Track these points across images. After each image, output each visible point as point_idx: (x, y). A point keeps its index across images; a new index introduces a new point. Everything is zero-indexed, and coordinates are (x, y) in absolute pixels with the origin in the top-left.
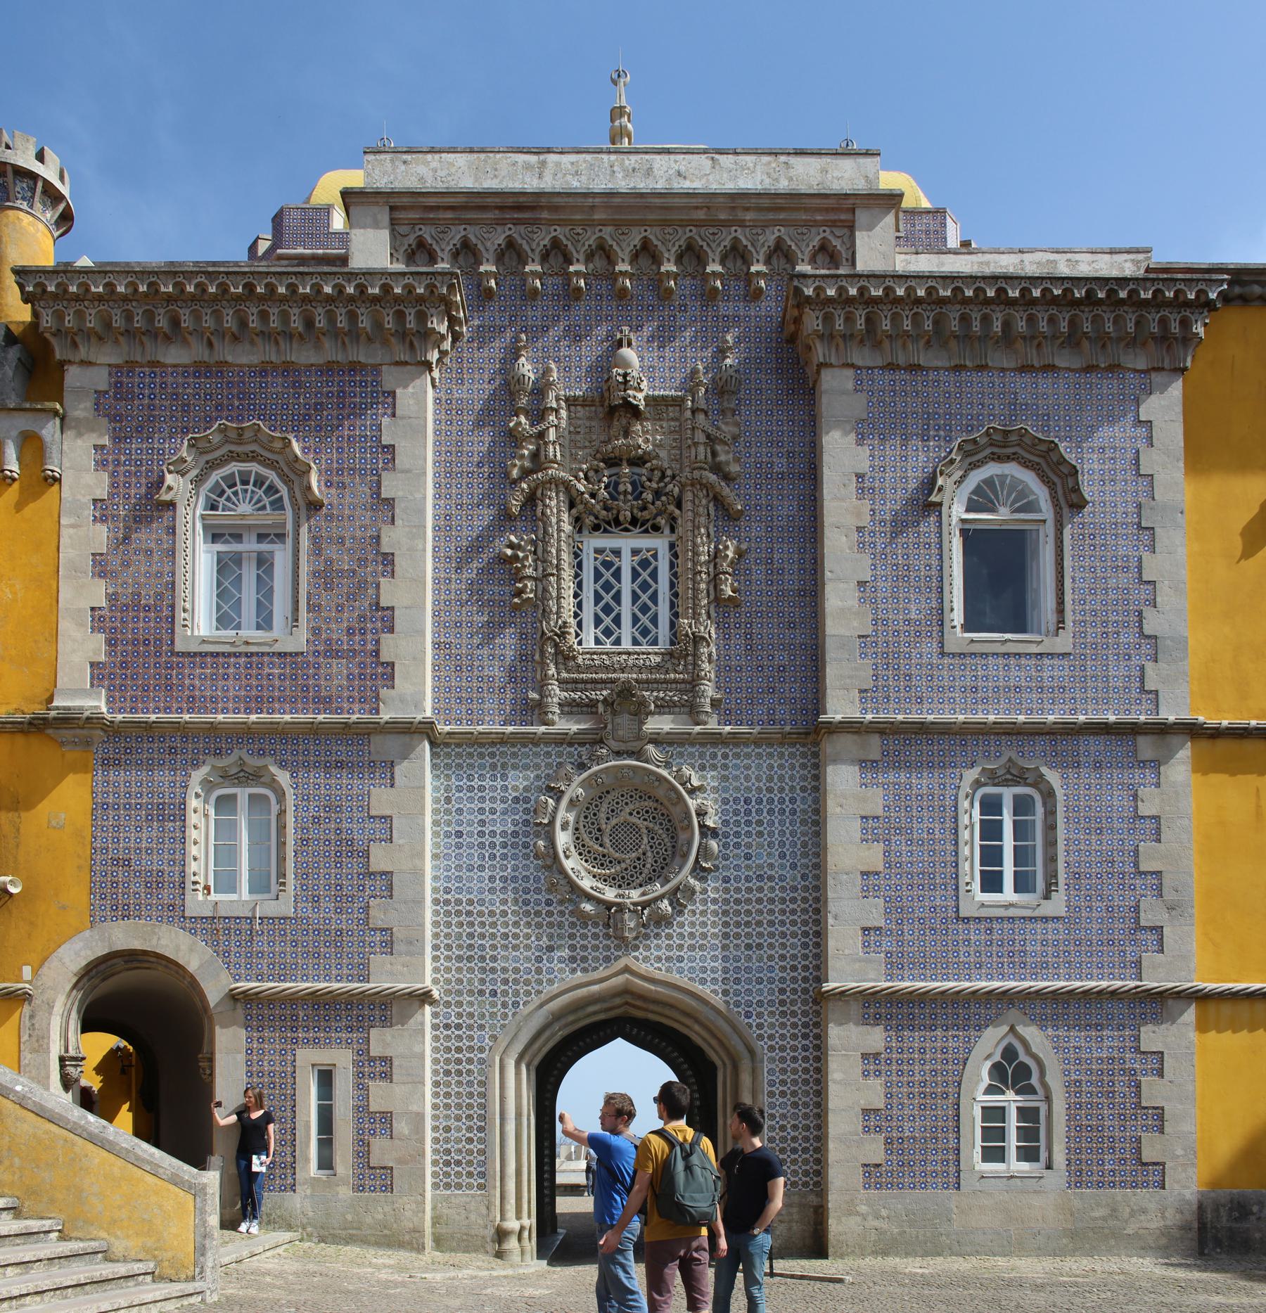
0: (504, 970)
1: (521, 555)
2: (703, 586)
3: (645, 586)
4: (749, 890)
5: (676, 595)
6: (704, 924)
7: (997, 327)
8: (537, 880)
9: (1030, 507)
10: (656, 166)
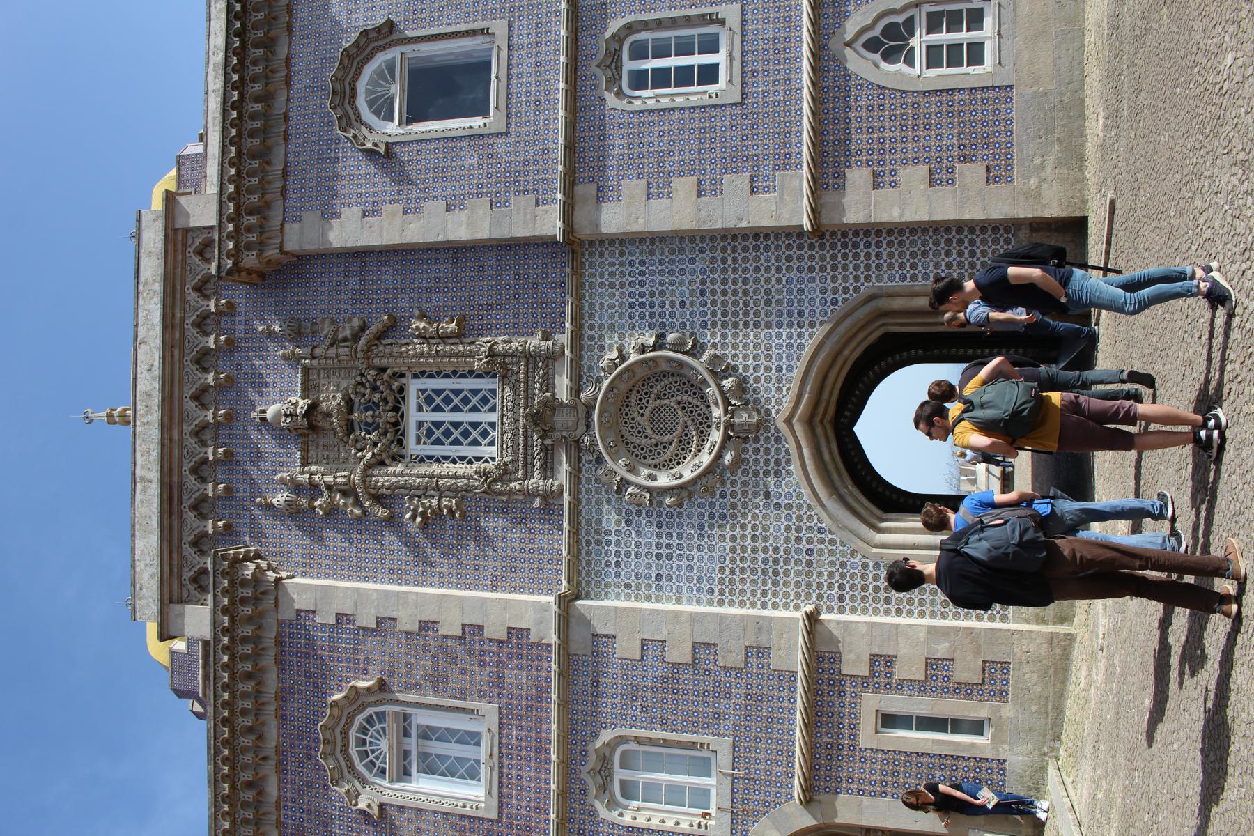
0: (787, 540)
1: (421, 509)
2: (448, 349)
3: (447, 400)
4: (714, 303)
5: (455, 372)
6: (746, 346)
7: (258, 107)
8: (702, 506)
9: (391, 67)
10: (144, 389)
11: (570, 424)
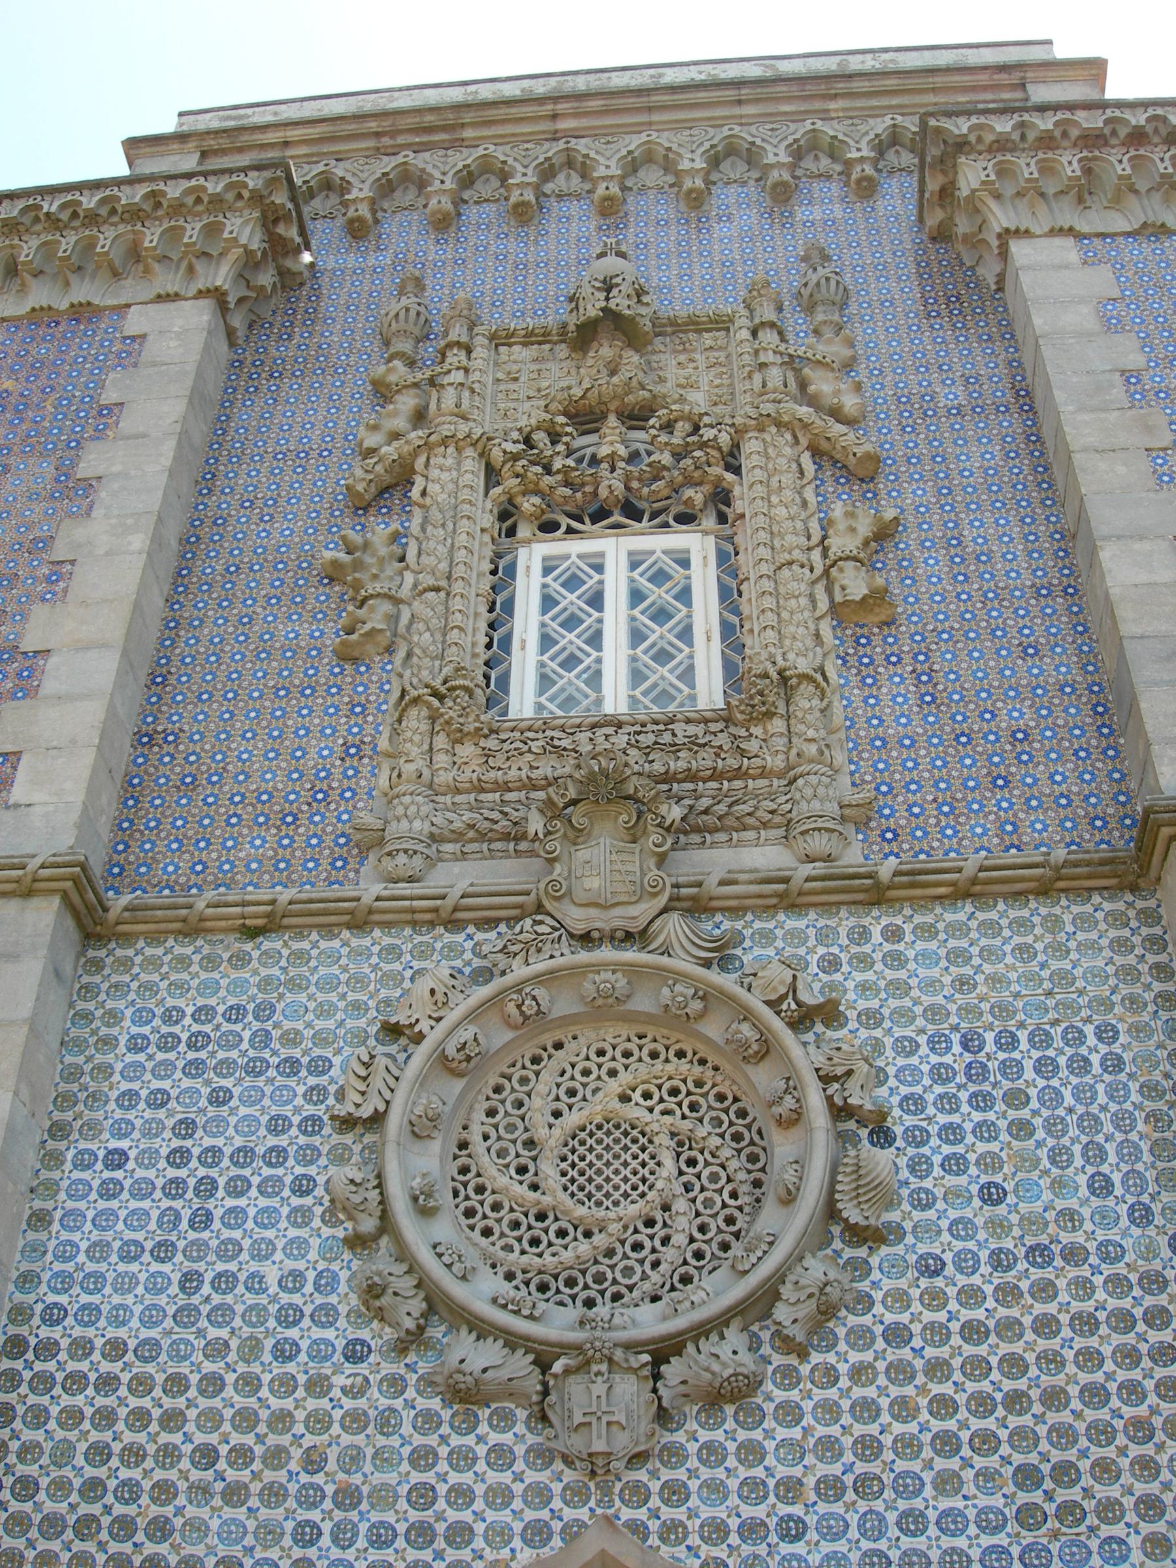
11: (594, 883)
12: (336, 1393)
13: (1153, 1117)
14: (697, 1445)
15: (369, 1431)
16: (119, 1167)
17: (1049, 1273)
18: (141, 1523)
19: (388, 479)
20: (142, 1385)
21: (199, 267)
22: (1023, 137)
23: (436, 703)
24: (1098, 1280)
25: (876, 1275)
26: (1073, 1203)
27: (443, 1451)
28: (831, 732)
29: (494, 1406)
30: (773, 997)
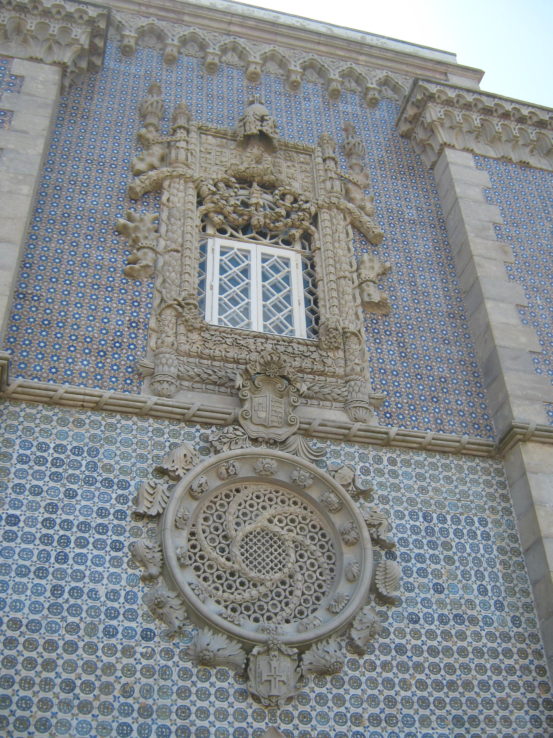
4: (446, 635)
8: (131, 598)
11: (263, 415)
12: (138, 656)
13: (503, 563)
14: (314, 695)
15: (156, 677)
16: (15, 524)
17: (463, 628)
18: (32, 721)
19: (149, 188)
20: (31, 645)
21: (55, 48)
22: (458, 102)
23: (180, 310)
24: (483, 633)
25: (390, 620)
26: (472, 597)
27: (194, 690)
28: (363, 362)
29: (218, 668)
30: (345, 483)
